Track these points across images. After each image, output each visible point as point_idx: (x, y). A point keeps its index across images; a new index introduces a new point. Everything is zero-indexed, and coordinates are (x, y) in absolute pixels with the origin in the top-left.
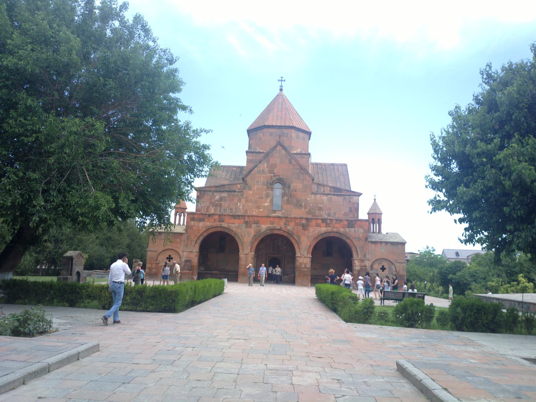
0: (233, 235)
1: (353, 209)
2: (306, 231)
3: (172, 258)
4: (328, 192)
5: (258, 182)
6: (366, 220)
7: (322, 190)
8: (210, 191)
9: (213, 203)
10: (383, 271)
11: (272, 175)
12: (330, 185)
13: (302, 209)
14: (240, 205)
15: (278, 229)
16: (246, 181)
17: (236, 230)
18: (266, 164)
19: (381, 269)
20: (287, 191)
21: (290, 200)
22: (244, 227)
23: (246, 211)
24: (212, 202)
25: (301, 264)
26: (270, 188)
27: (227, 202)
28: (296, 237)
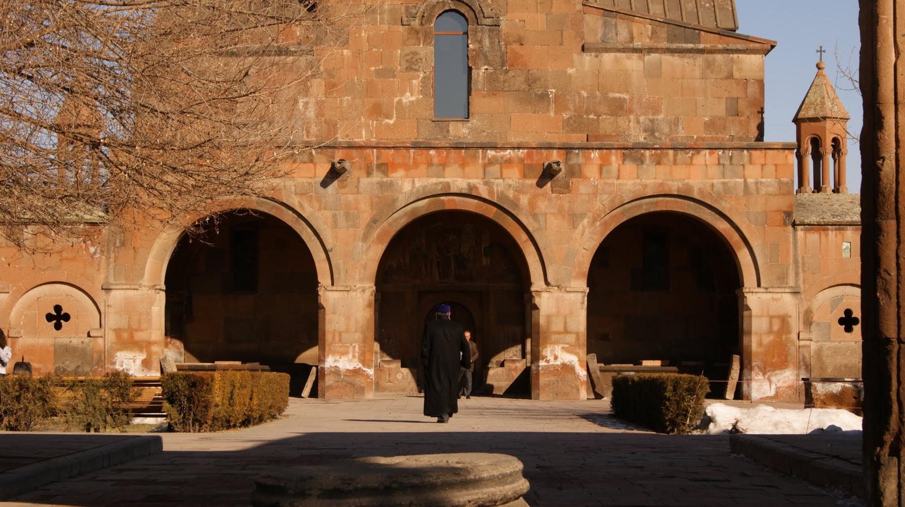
0: (290, 224)
1: (740, 101)
2: (566, 196)
3: (67, 317)
4: (647, 42)
6: (786, 148)
7: (623, 34)
10: (848, 329)
12: (656, 10)
13: (548, 111)
14: (306, 104)
17: (301, 205)
19: (841, 321)
20: (487, 42)
21: (502, 78)
23: (332, 126)
25: (549, 317)
26: (420, 34)
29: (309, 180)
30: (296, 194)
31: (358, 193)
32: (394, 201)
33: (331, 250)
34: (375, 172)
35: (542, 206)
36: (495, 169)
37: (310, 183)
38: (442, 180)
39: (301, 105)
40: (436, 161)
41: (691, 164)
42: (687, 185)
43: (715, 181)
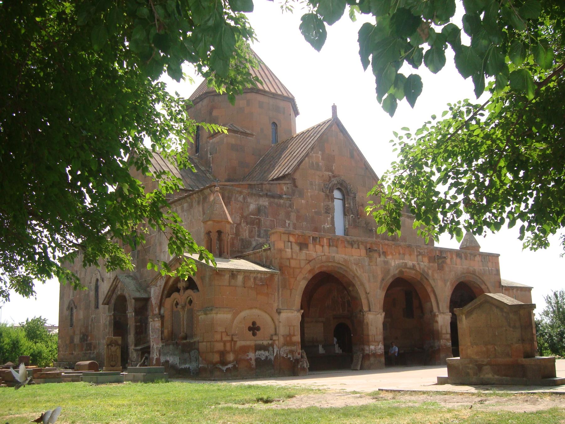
3: (258, 329)
5: (311, 184)
8: (241, 193)
9: (245, 218)
11: (330, 174)
14: (289, 224)
15: (410, 268)
16: (294, 180)
17: (356, 270)
18: (320, 152)
20: (352, 203)
22: (367, 264)
24: (245, 214)
26: (330, 198)
27: (270, 218)
28: (431, 282)
29: (359, 258)
30: (354, 264)
31: (376, 265)
32: (389, 270)
33: (369, 293)
34: (382, 256)
35: (436, 275)
36: (420, 257)
37: (359, 259)
38: (404, 261)
39: (287, 224)
40: (401, 252)
41: (474, 260)
42: (475, 269)
43: (481, 268)
